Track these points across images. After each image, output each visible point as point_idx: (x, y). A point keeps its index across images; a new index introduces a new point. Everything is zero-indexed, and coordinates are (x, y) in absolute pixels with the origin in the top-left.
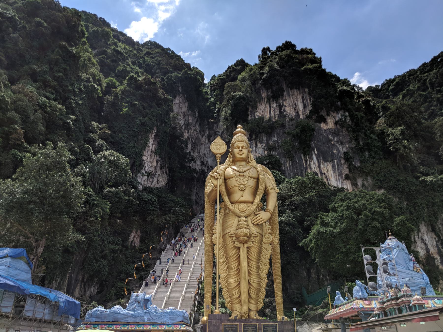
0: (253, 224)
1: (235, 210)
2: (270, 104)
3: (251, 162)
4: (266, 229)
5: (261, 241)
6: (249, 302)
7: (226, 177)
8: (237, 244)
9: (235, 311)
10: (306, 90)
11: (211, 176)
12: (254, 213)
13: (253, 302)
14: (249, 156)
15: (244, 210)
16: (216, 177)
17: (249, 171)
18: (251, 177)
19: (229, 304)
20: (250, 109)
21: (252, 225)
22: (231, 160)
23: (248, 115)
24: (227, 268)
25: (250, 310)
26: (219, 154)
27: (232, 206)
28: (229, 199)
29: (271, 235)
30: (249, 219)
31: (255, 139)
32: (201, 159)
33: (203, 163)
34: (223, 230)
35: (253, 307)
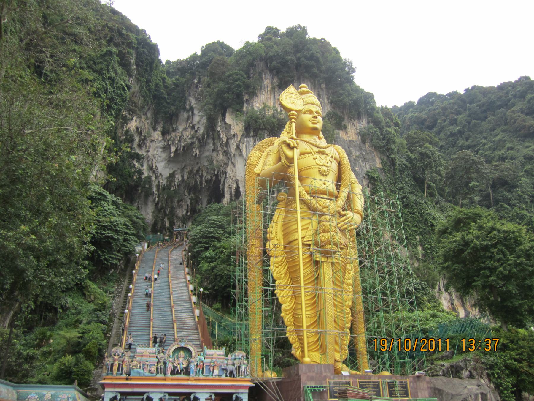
2: (274, 96)
10: (323, 86)
12: (339, 213)
13: (337, 348)
19: (299, 351)
20: (246, 97)
23: (243, 103)
25: (336, 361)
26: (296, 111)
31: (253, 136)
32: (148, 161)
33: (151, 168)
35: (338, 356)
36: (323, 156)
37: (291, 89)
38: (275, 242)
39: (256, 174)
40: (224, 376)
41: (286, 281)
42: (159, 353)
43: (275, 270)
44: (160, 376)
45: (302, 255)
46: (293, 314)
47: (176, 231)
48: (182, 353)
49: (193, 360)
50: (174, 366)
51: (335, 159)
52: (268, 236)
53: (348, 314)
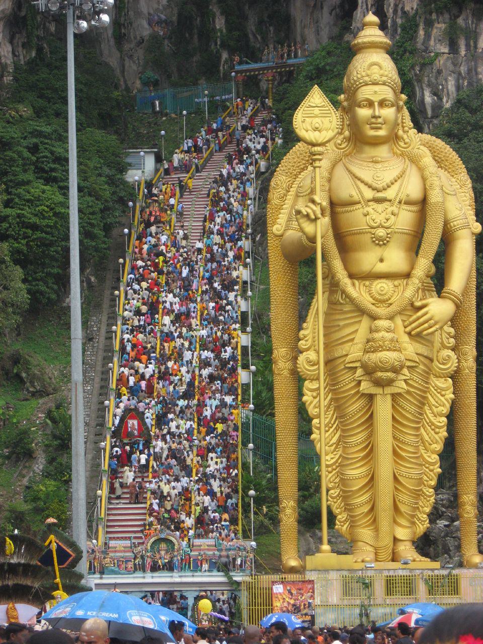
0: (409, 334)
1: (361, 299)
3: (405, 137)
4: (442, 339)
5: (428, 372)
6: (395, 522)
7: (335, 199)
8: (366, 387)
9: (360, 544)
11: (299, 212)
12: (412, 305)
14: (400, 121)
15: (386, 297)
16: (313, 217)
17: (399, 182)
18: (405, 203)
19: (345, 526)
21: (406, 338)
22: (347, 133)
24: (339, 440)
25: (396, 540)
27: (354, 285)
28: (346, 267)
29: (451, 353)
30: (399, 320)
34: (326, 346)
35: (403, 533)
36: (380, 207)
37: (316, 97)
38: (312, 355)
39: (277, 236)
40: (215, 573)
41: (328, 420)
42: (135, 547)
43: (311, 402)
44: (139, 574)
45: (347, 381)
46: (338, 471)
47: (241, 72)
48: (163, 546)
49: (176, 553)
50: (154, 561)
51: (408, 203)
52: (302, 344)
53: (433, 464)
